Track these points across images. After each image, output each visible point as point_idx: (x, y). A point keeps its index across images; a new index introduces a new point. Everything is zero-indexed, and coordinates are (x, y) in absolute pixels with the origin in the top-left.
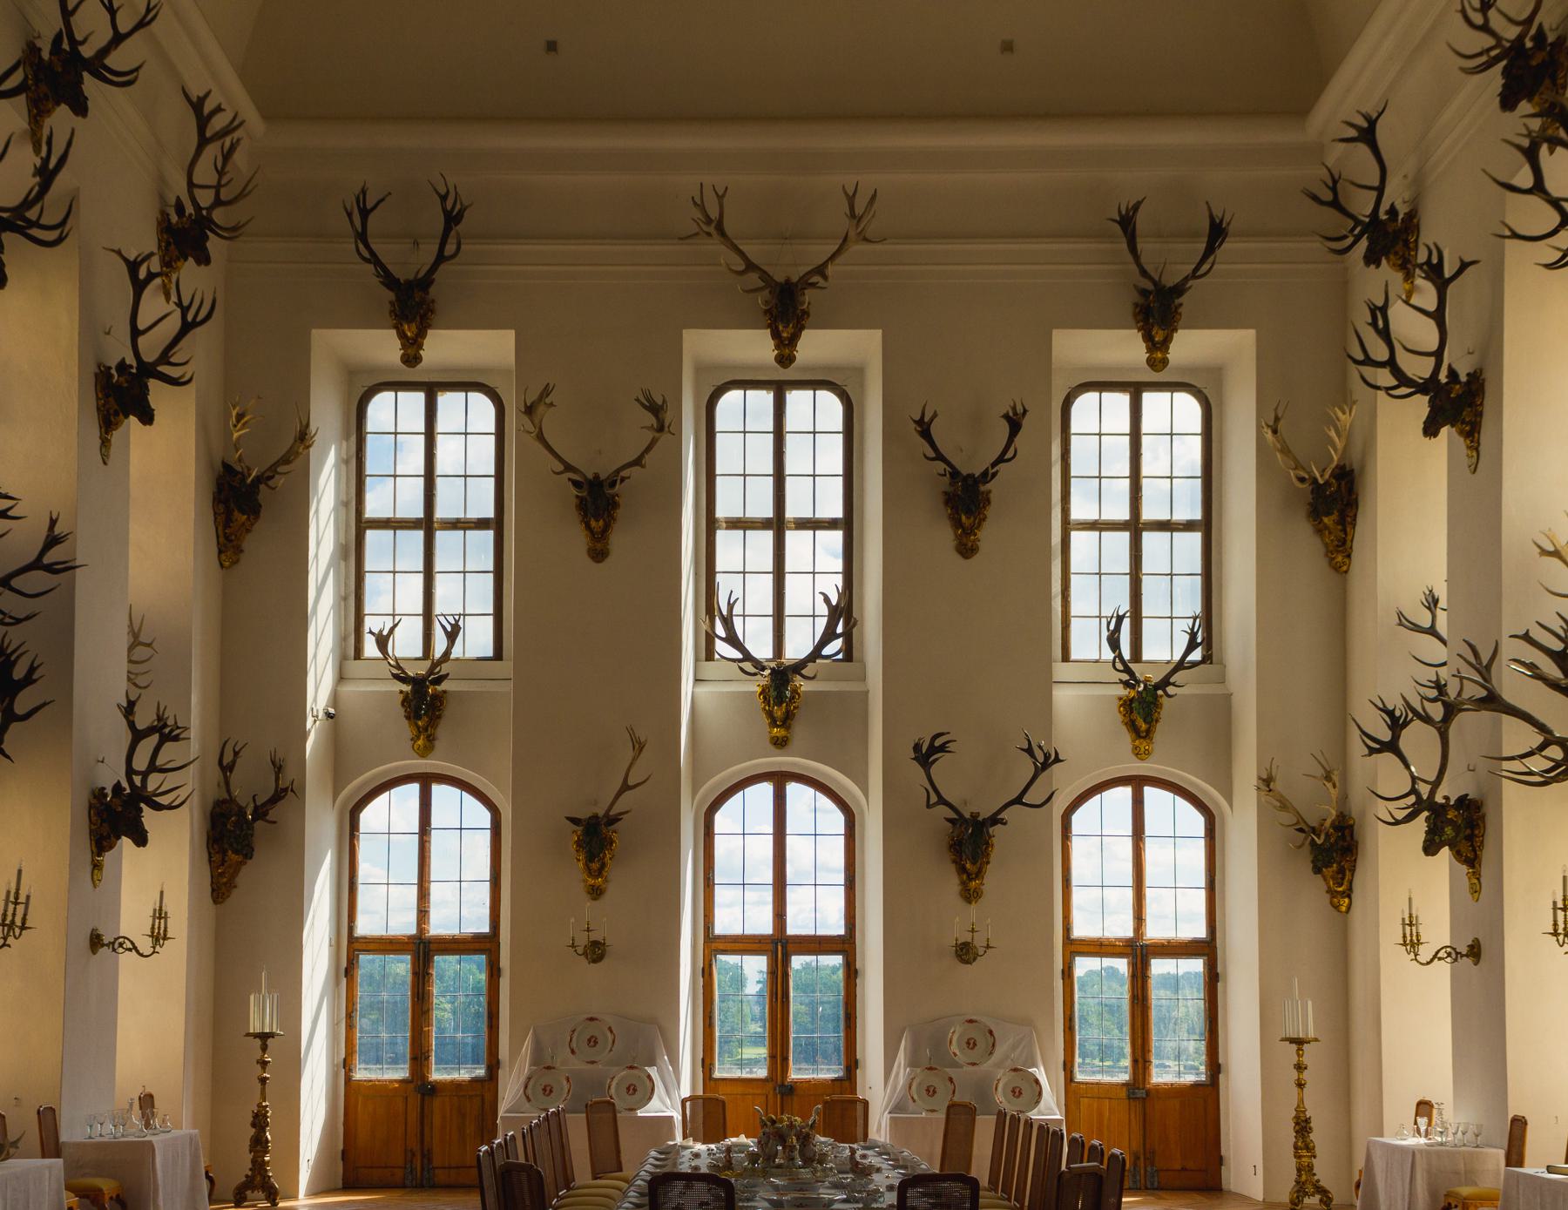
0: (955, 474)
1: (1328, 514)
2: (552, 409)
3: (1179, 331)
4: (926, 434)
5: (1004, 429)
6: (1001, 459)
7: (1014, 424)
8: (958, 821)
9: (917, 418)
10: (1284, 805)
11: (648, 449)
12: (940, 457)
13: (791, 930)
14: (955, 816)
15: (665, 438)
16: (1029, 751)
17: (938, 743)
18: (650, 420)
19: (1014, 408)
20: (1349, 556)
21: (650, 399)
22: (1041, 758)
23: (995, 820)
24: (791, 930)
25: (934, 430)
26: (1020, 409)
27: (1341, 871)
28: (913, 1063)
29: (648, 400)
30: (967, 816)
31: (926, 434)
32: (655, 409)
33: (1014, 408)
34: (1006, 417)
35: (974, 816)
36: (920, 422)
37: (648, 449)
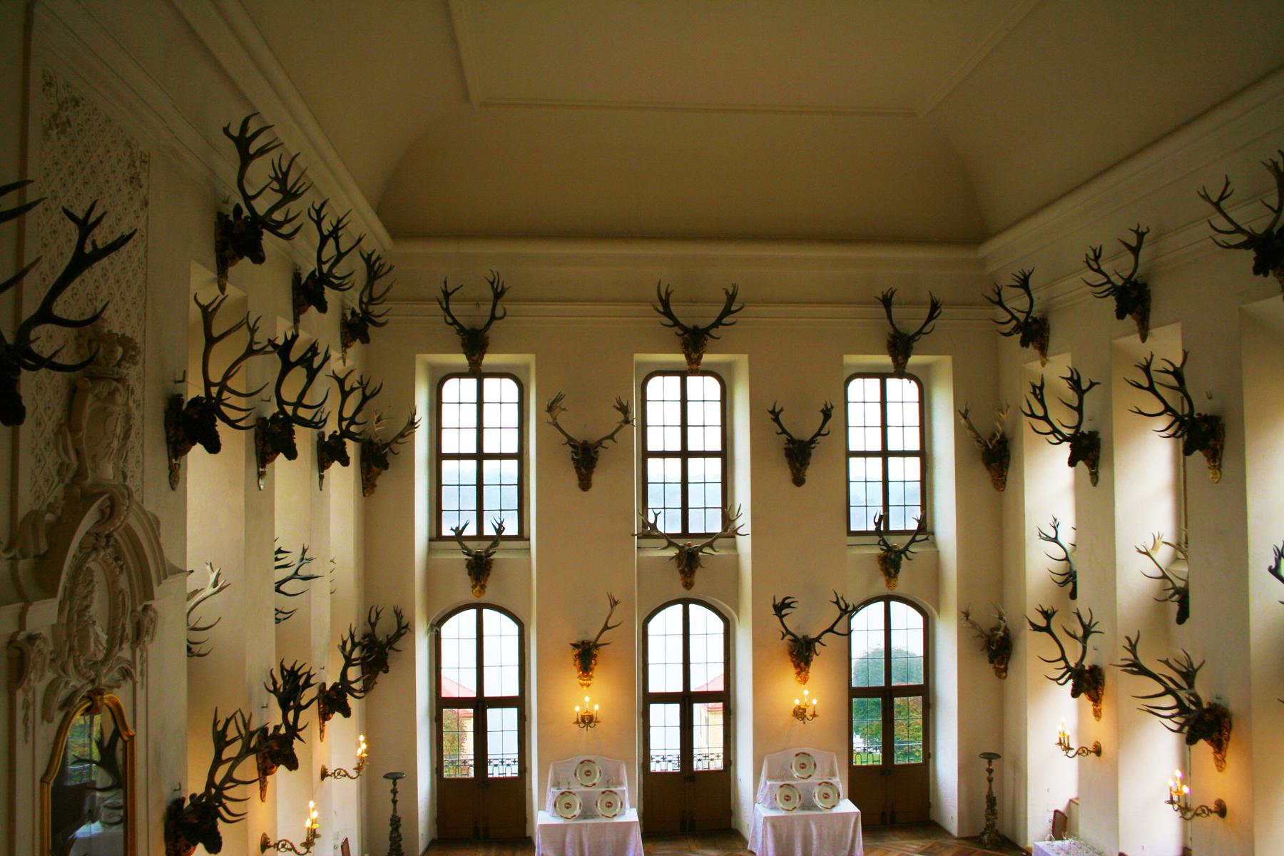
0: (791, 440)
1: (994, 462)
2: (563, 412)
3: (912, 356)
4: (777, 420)
5: (821, 416)
6: (818, 434)
7: (827, 414)
8: (795, 640)
9: (771, 409)
10: (974, 624)
11: (617, 430)
12: (784, 432)
13: (693, 689)
14: (793, 638)
15: (627, 426)
16: (837, 603)
17: (787, 601)
18: (621, 416)
19: (826, 406)
20: (1004, 483)
21: (620, 403)
22: (843, 607)
23: (818, 639)
24: (693, 689)
25: (781, 417)
26: (829, 407)
27: (1003, 659)
28: (770, 777)
29: (619, 404)
30: (800, 636)
31: (777, 420)
32: (625, 410)
33: (826, 406)
34: (822, 411)
35: (805, 637)
36: (773, 412)
37: (617, 430)
